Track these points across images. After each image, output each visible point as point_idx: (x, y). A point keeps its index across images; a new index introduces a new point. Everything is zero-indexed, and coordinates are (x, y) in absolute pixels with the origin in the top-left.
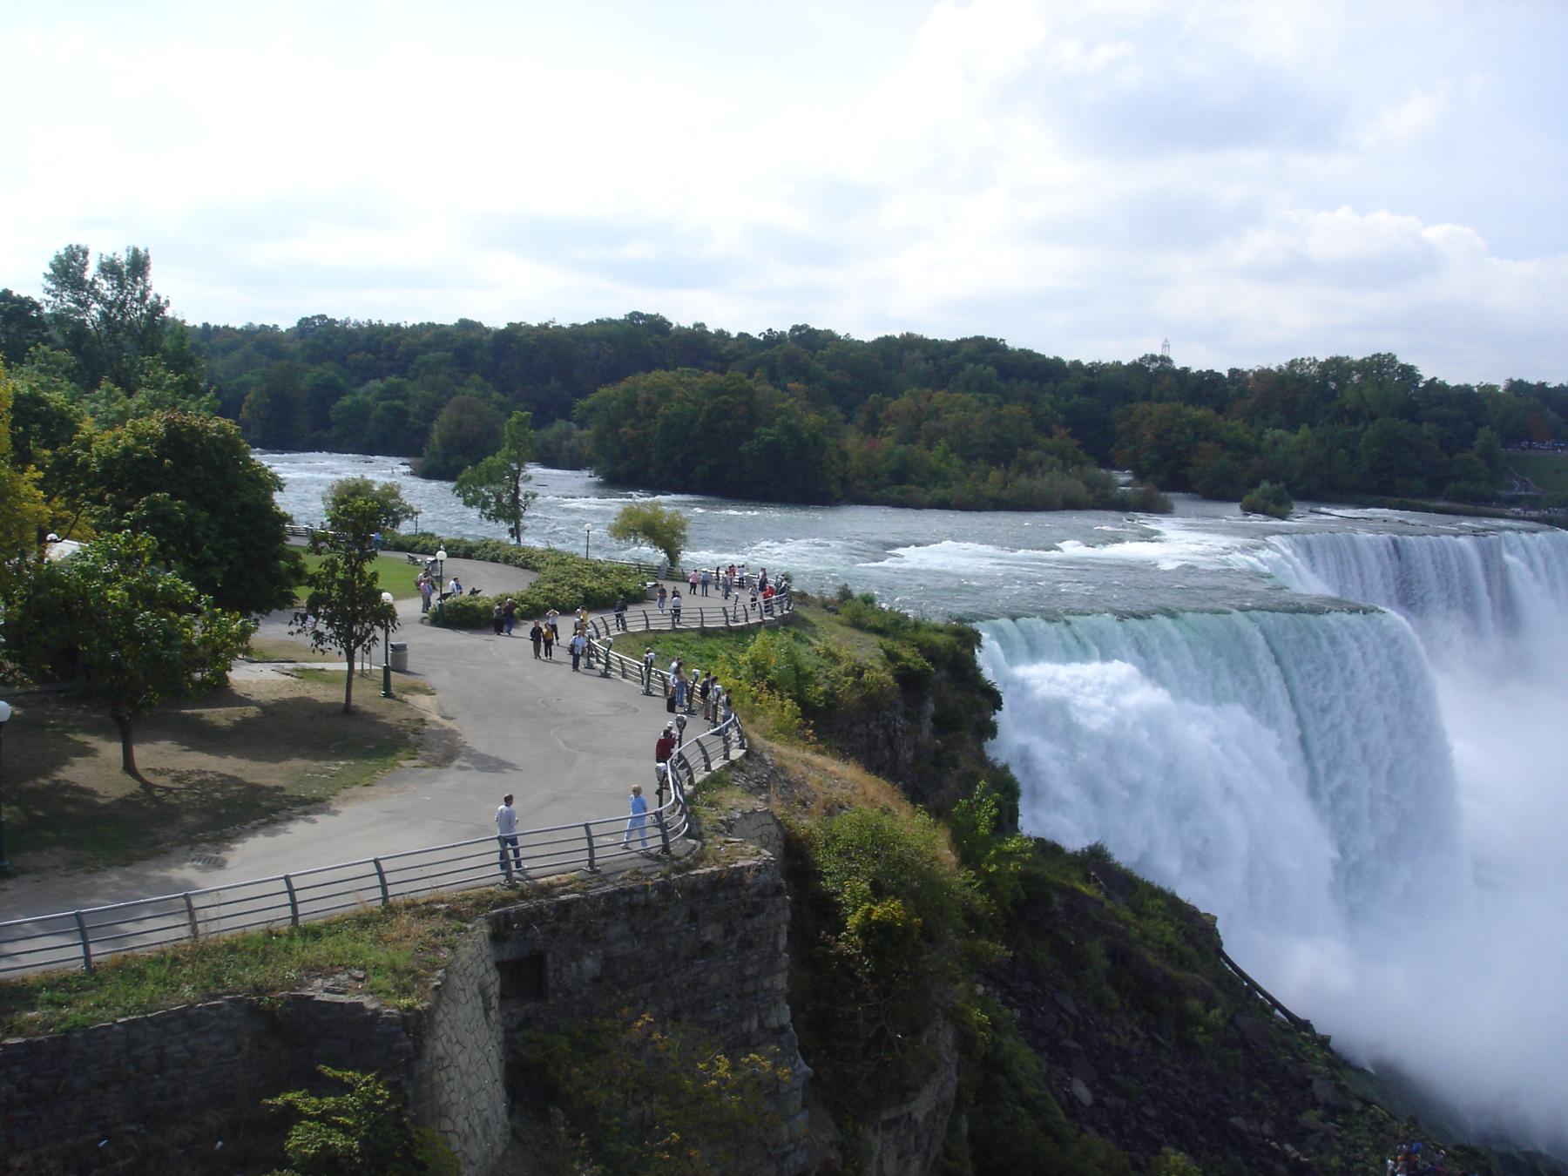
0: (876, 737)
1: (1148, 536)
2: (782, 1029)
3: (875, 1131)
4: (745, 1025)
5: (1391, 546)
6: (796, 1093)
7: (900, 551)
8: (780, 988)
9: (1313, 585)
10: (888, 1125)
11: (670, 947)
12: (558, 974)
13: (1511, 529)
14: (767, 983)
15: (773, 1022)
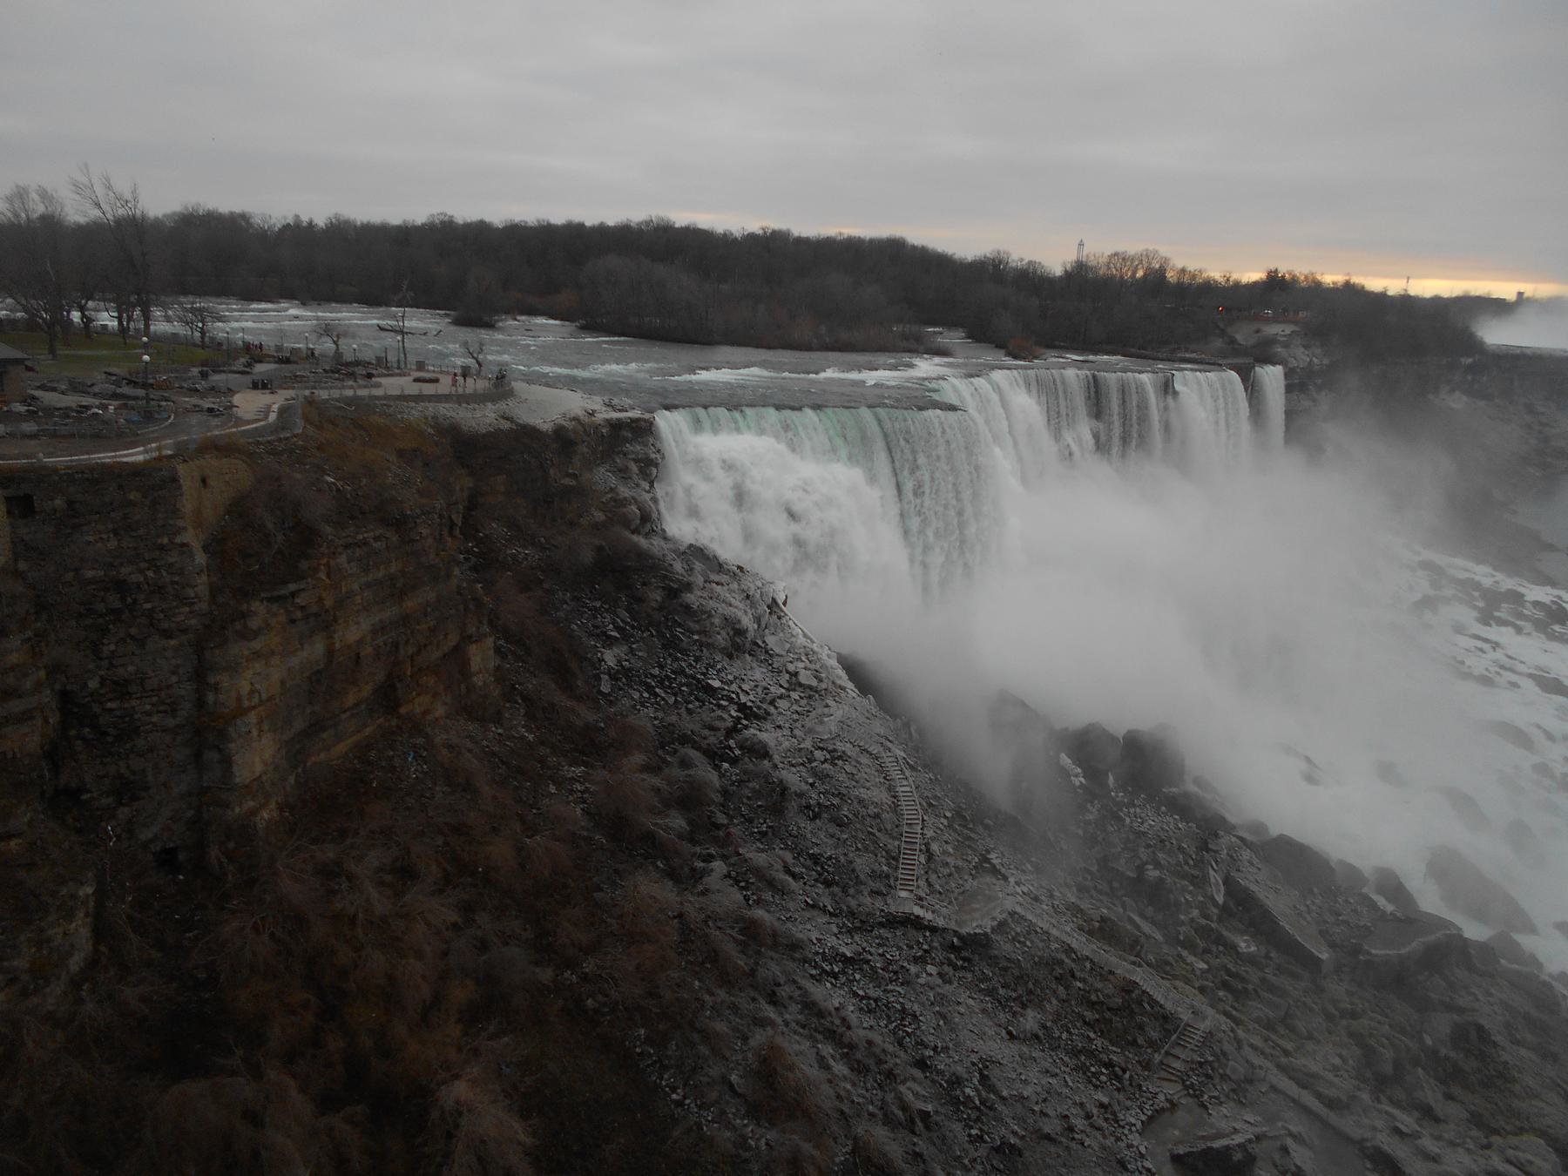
7: (702, 372)
14: (171, 522)
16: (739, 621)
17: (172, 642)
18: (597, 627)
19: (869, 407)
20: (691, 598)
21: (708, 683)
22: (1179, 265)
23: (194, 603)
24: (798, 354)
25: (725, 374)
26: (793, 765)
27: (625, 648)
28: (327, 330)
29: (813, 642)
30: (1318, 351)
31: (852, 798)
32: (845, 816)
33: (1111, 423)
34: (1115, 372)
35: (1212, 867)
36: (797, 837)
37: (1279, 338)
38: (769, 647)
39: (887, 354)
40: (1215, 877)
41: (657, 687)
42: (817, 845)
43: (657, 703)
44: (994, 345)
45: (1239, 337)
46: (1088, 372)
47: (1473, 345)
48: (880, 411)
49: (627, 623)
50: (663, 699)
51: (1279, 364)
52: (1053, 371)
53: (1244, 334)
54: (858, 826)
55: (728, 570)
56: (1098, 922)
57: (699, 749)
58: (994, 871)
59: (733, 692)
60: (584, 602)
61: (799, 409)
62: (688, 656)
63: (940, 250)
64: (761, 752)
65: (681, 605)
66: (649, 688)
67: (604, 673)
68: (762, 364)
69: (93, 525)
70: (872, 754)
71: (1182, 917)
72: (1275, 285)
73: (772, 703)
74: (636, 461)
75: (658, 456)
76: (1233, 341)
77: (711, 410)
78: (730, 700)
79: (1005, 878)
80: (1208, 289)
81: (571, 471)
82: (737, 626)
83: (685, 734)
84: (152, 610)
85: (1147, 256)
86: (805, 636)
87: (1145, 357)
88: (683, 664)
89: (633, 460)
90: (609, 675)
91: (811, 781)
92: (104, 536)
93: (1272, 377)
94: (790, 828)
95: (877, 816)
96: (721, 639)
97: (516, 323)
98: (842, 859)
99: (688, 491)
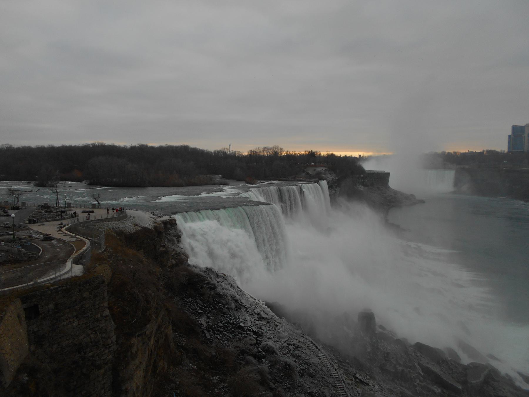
0: (150, 243)
2: (107, 316)
3: (135, 337)
4: (97, 316)
5: (278, 189)
6: (112, 331)
8: (105, 306)
9: (262, 199)
10: (139, 336)
11: (74, 299)
12: (42, 310)
13: (305, 184)
14: (102, 305)
15: (104, 314)
16: (235, 297)
17: (102, 371)
18: (193, 310)
20: (219, 290)
21: (240, 325)
22: (286, 150)
23: (110, 347)
24: (180, 188)
25: (172, 198)
26: (285, 354)
27: (205, 317)
28: (12, 192)
29: (255, 299)
30: (334, 175)
31: (311, 364)
32: (312, 372)
33: (286, 203)
34: (285, 186)
35: (415, 361)
36: (301, 386)
37: (322, 172)
38: (245, 304)
39: (209, 186)
40: (416, 364)
41: (224, 331)
42: (309, 388)
43: (227, 338)
44: (236, 180)
45: (310, 172)
46: (277, 187)
47: (362, 170)
48: (244, 207)
49: (202, 306)
50: (228, 336)
51: (325, 180)
52: (267, 187)
53: (311, 171)
54: (318, 376)
55: (220, 276)
56: (400, 394)
57: (250, 355)
58: (361, 382)
59: (249, 327)
60: (185, 300)
62: (227, 315)
63: (201, 148)
64: (270, 351)
65: (217, 294)
66: (221, 332)
67: (205, 330)
68: (182, 194)
69: (66, 315)
70: (302, 342)
71: (415, 384)
72: (312, 155)
73: (260, 328)
74: (175, 236)
75: (181, 234)
76: (308, 174)
77: (189, 213)
78: (250, 330)
79: (368, 385)
80: (291, 158)
81: (162, 244)
82: (235, 299)
83: (243, 350)
84: (93, 356)
85: (275, 148)
86: (251, 297)
87: (286, 180)
88: (227, 319)
89: (173, 236)
90: (206, 330)
91: (294, 360)
92: (72, 320)
93: (324, 183)
94: (297, 383)
95: (321, 369)
96: (233, 305)
97: (60, 184)
98: (319, 392)
99: (190, 244)
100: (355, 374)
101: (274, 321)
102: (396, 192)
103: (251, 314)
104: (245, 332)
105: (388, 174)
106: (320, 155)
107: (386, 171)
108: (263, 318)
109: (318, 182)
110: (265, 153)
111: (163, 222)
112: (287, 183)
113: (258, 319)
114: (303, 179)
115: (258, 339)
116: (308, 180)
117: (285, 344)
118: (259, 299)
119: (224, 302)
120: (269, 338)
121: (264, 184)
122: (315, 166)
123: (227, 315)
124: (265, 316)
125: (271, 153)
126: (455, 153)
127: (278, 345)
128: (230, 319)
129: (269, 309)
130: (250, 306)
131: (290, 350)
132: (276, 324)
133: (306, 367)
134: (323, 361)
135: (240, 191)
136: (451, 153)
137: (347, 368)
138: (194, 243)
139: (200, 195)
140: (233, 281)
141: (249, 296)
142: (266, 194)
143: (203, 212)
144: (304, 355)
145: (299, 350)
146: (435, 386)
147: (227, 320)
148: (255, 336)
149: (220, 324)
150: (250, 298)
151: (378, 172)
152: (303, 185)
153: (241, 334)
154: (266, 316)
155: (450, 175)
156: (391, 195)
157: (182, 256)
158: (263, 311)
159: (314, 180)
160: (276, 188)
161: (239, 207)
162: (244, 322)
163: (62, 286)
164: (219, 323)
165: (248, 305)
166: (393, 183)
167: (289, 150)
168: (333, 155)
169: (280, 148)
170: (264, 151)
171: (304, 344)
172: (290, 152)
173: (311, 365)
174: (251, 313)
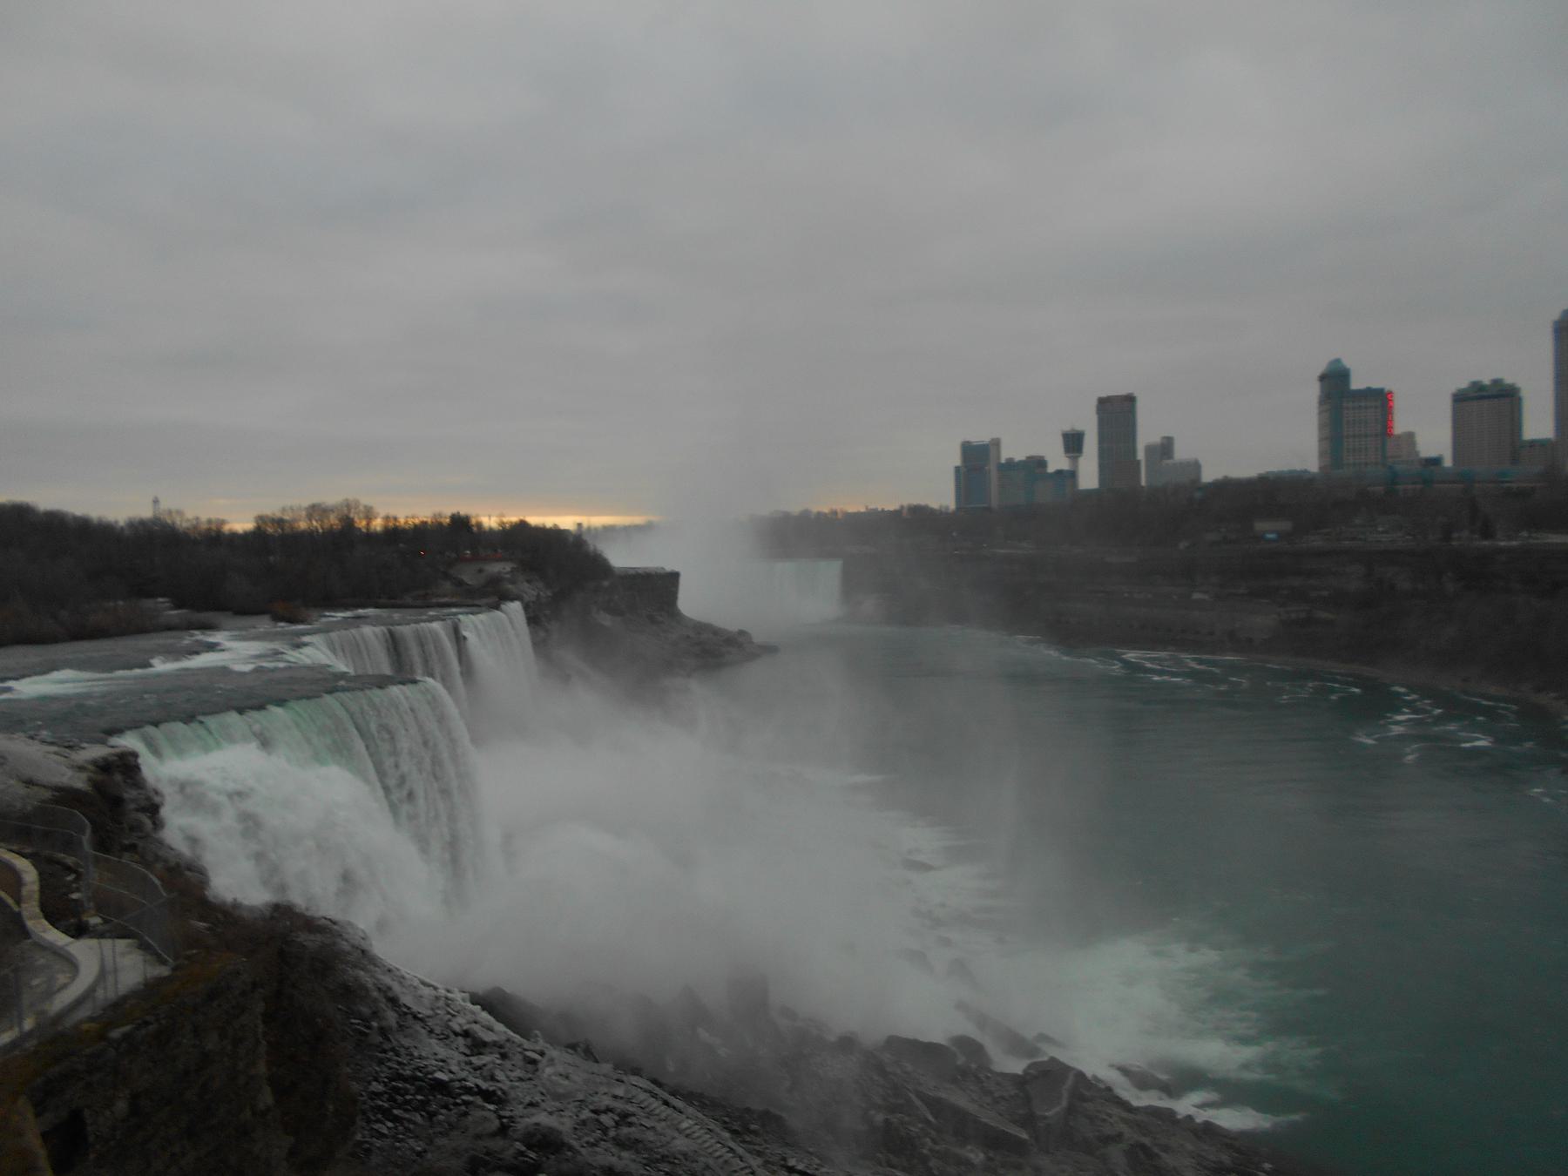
1: (212, 647)
5: (388, 635)
13: (461, 613)
16: (390, 988)
19: (327, 693)
29: (436, 988)
34: (408, 624)
50: (410, 1121)
53: (469, 575)
61: (261, 707)
66: (387, 1114)
72: (460, 524)
74: (143, 810)
76: (460, 583)
78: (468, 1091)
81: (126, 842)
82: (390, 994)
86: (423, 983)
89: (137, 810)
93: (515, 607)
100: (784, 1159)
101: (519, 1050)
102: (701, 628)
103: (443, 1038)
104: (455, 1098)
105: (674, 577)
106: (479, 525)
107: (669, 568)
108: (485, 1044)
109: (497, 607)
110: (314, 523)
111: (97, 767)
112: (409, 614)
113: (468, 1052)
114: (454, 600)
115: (502, 1113)
116: (470, 602)
117: (586, 1114)
118: (449, 987)
119: (365, 1010)
120: (531, 1104)
121: (335, 619)
122: (476, 558)
123: (385, 1051)
124: (488, 1037)
125: (333, 520)
126: (835, 513)
127: (565, 1120)
128: (400, 1063)
129: (485, 1016)
130: (430, 1013)
131: (605, 1130)
132: (528, 1057)
133: (666, 1169)
134: (700, 1141)
135: (276, 645)
136: (825, 514)
137: (757, 1148)
138: (203, 825)
139: (151, 666)
140: (363, 939)
141: (416, 983)
142: (355, 650)
143: (212, 722)
144: (650, 1136)
145: (630, 1125)
146: (969, 1147)
147: (390, 1068)
148: (492, 1107)
149: (377, 1087)
150: (422, 986)
151: (647, 571)
152: (461, 617)
153: (446, 1107)
154: (495, 1038)
155: (830, 573)
156: (688, 637)
157: (188, 873)
158: (476, 1022)
159: (484, 601)
160: (382, 631)
161: (325, 695)
162: (442, 1067)
163: (147, 1023)
164: (369, 1083)
165: (426, 1012)
166: (691, 602)
167: (392, 512)
168: (523, 525)
169: (365, 507)
170: (310, 517)
171: (629, 1101)
172: (395, 519)
173: (676, 1161)
174: (443, 1034)
